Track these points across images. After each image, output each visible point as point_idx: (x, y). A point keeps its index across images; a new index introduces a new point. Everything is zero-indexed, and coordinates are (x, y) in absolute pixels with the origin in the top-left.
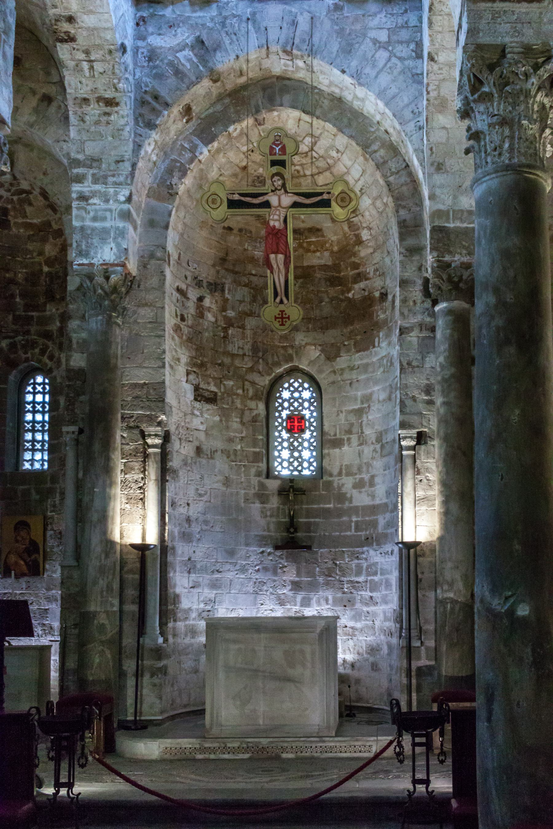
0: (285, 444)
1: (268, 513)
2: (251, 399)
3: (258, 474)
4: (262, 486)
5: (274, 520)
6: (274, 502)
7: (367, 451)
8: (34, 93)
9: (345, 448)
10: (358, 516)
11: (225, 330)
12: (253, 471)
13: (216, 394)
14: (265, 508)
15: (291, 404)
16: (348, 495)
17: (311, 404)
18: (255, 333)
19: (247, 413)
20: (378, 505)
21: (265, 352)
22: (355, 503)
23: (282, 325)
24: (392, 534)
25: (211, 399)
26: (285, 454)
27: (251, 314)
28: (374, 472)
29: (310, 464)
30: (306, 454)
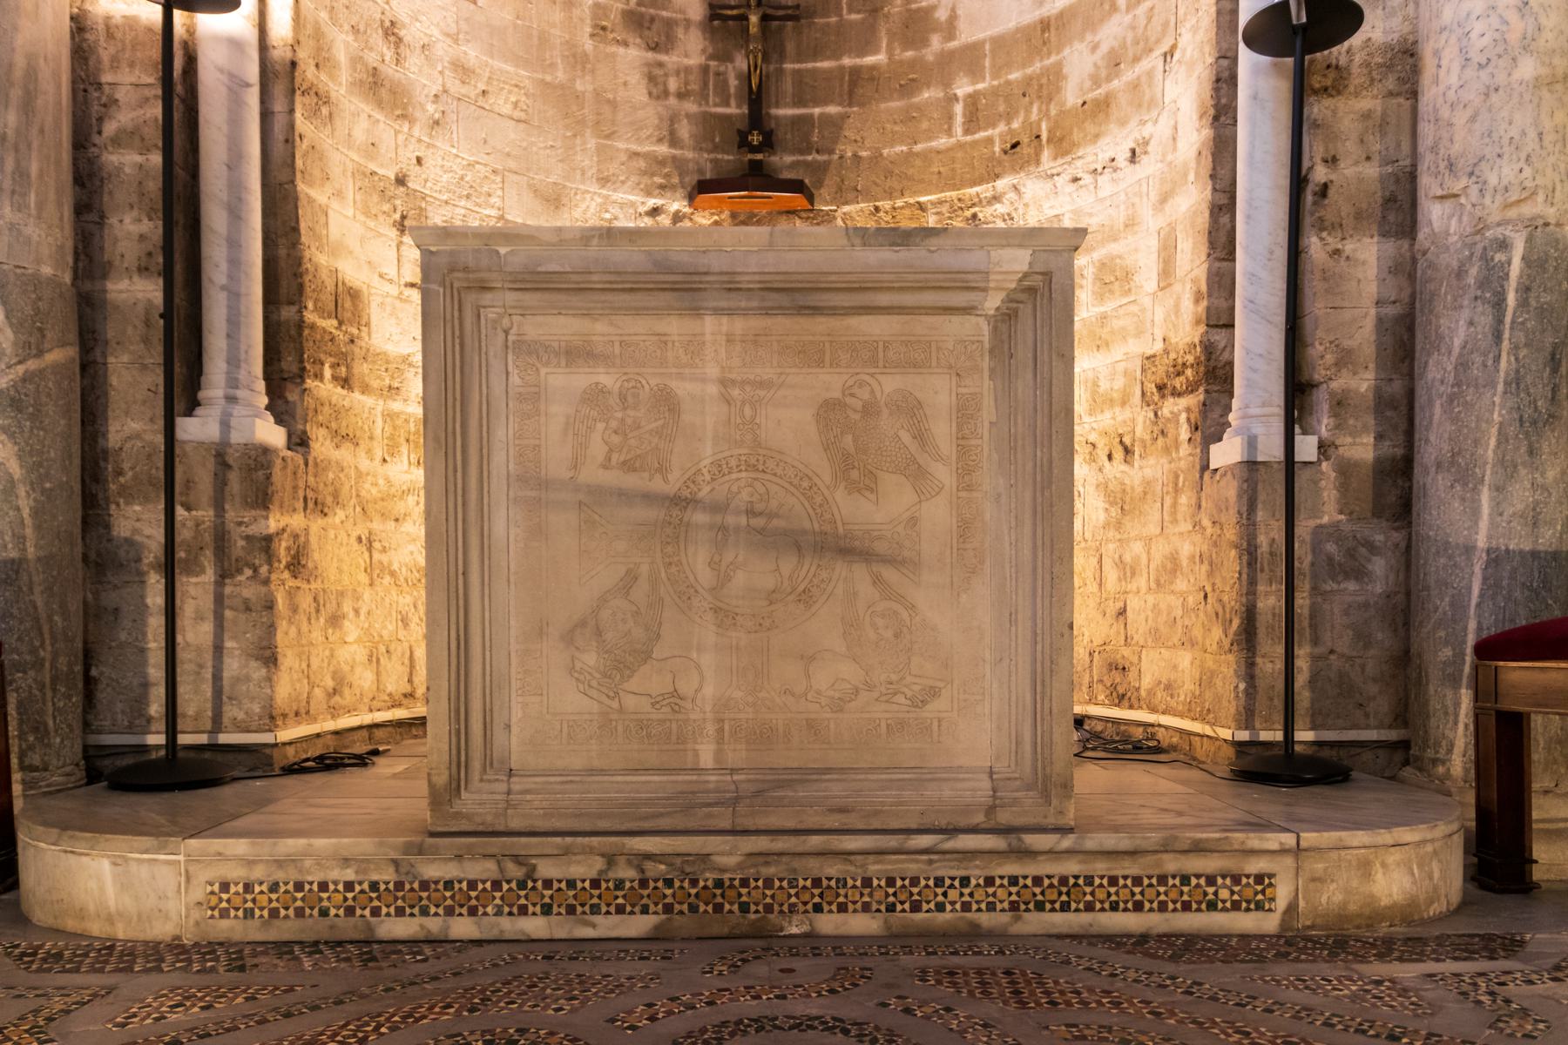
1: (673, 85)
5: (691, 107)
6: (692, 50)
10: (975, 73)
14: (660, 65)
16: (942, 15)
20: (1061, 15)
22: (967, 35)
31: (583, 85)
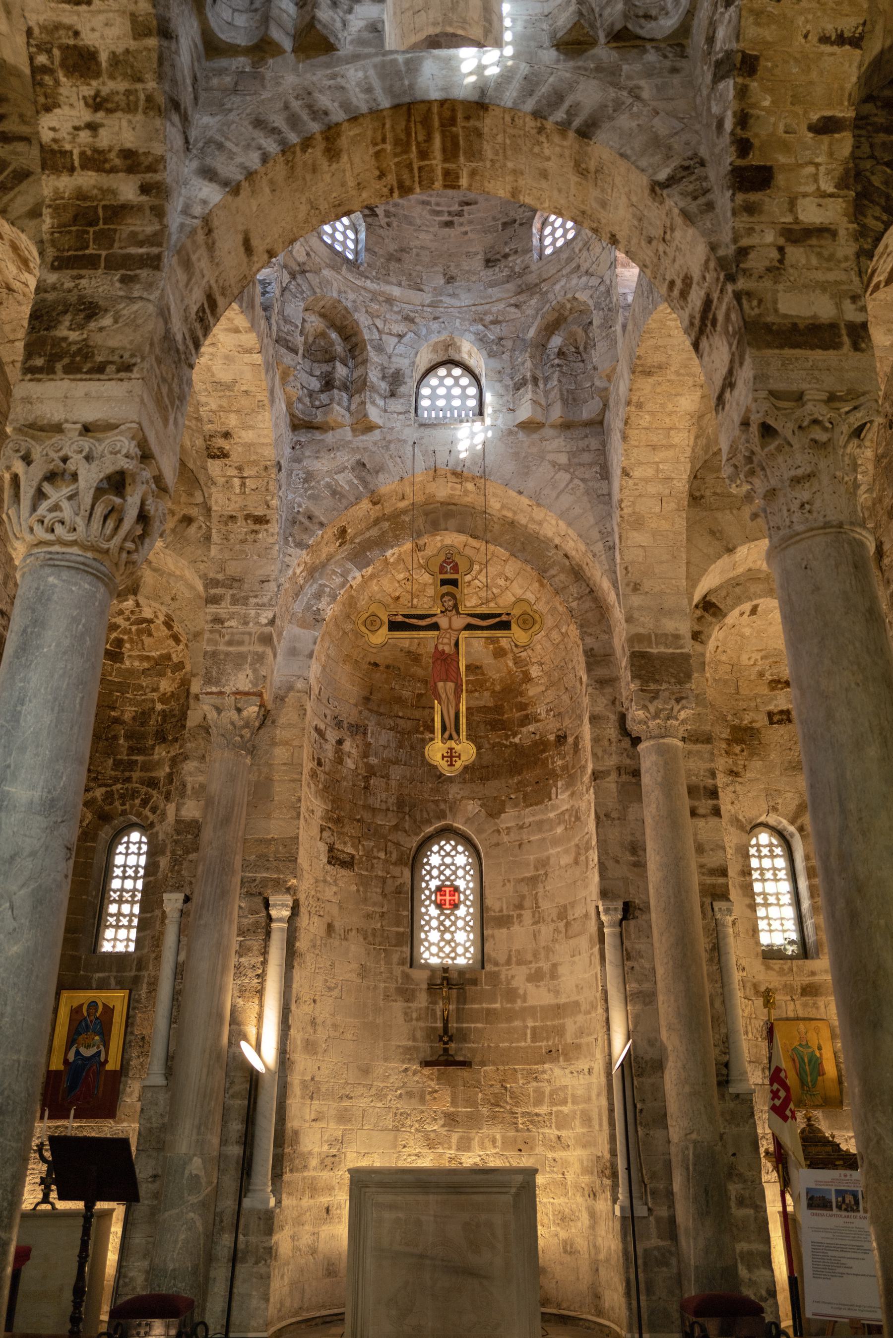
0: (434, 923)
1: (414, 1015)
2: (395, 864)
3: (402, 963)
4: (406, 977)
5: (422, 1024)
6: (422, 1000)
7: (546, 931)
8: (173, 513)
9: (516, 928)
11: (367, 779)
12: (395, 957)
13: (353, 856)
15: (441, 873)
16: (521, 992)
17: (467, 872)
18: (401, 785)
19: (389, 882)
21: (413, 806)
22: (531, 1002)
23: (451, 765)
24: (588, 1044)
25: (347, 863)
26: (434, 936)
27: (397, 762)
28: (555, 959)
29: (467, 950)
30: (461, 937)
31: (379, 1021)
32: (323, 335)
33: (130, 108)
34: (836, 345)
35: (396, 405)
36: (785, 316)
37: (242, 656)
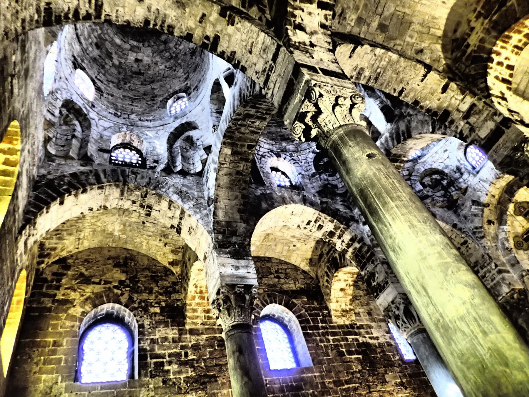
32: (432, 179)
33: (344, 233)
34: (503, 132)
35: (465, 176)
36: (485, 138)
37: (498, 282)
